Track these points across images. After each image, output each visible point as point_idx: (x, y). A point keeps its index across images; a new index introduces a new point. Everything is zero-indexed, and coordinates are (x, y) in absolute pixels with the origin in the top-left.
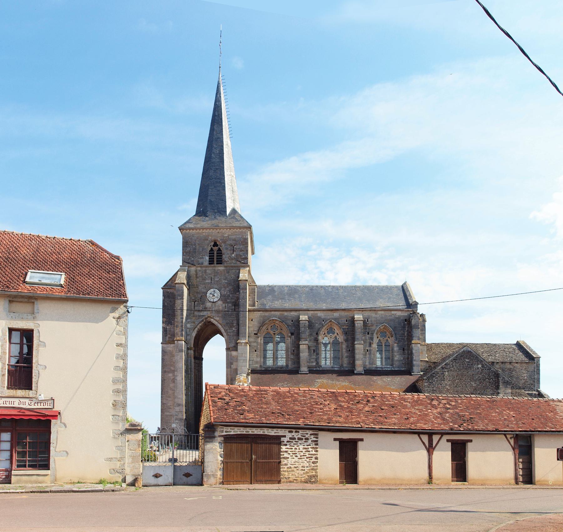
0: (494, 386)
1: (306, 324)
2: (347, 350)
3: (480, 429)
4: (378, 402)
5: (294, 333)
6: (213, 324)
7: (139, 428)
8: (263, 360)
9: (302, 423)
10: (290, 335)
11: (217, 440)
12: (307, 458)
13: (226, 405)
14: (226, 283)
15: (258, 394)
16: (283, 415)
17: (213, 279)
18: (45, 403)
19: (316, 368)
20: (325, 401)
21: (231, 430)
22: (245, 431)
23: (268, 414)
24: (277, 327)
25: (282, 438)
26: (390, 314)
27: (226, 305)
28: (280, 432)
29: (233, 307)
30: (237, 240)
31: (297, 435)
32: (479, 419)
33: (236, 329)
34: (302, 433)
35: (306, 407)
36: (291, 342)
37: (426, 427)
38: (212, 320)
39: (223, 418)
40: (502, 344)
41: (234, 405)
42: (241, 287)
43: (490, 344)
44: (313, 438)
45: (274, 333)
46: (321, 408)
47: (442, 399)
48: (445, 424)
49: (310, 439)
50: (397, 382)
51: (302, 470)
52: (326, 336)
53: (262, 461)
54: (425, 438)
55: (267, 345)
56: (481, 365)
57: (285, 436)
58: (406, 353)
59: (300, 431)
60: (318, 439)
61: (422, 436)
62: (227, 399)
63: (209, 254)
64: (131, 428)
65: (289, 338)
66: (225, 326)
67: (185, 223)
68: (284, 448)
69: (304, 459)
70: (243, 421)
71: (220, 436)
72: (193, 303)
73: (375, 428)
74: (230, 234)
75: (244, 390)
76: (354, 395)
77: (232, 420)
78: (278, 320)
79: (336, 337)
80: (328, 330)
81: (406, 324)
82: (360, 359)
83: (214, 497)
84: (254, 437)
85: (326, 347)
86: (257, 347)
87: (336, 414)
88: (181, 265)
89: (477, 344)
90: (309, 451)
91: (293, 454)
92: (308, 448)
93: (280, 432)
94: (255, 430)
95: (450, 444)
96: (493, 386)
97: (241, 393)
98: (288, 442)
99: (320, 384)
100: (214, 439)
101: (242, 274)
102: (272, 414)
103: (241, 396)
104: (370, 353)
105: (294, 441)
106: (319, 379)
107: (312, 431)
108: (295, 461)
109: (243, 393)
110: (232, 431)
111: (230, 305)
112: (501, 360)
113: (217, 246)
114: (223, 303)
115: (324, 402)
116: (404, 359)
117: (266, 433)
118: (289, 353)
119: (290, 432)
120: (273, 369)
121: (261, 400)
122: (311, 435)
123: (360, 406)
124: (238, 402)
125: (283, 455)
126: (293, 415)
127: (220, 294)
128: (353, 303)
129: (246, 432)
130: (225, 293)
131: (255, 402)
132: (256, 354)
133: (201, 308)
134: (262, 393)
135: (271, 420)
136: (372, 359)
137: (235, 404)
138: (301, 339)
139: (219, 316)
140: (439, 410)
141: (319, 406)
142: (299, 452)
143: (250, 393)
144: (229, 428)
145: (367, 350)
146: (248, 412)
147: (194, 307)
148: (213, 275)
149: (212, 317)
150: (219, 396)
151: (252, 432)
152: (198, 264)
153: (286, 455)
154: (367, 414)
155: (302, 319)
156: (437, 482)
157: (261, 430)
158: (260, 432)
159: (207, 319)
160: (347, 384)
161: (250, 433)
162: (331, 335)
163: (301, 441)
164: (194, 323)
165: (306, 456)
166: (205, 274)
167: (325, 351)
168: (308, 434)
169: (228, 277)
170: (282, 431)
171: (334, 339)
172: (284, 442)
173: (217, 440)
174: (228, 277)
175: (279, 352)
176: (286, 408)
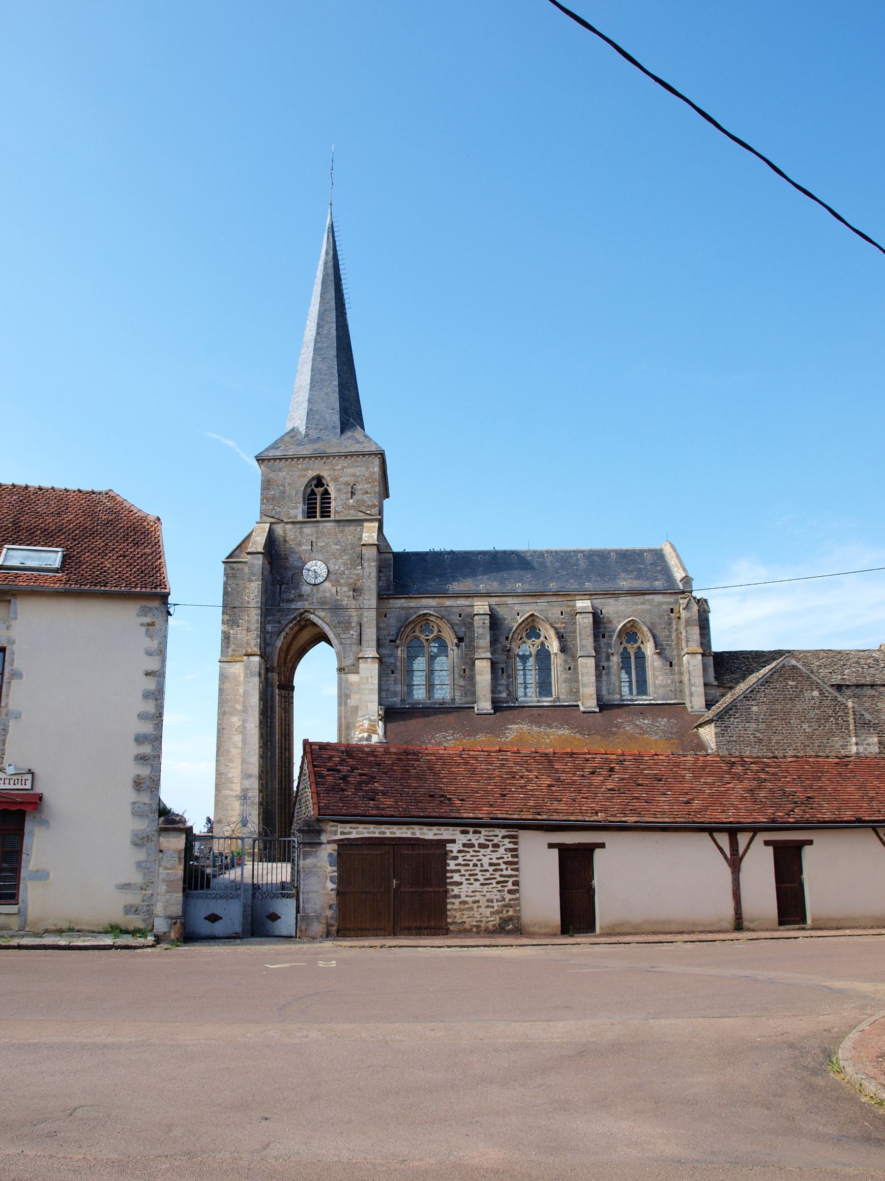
0: (846, 731)
1: (486, 622)
2: (565, 669)
3: (826, 819)
4: (631, 771)
5: (463, 638)
6: (315, 625)
7: (181, 826)
8: (407, 690)
9: (487, 816)
10: (456, 641)
11: (326, 849)
12: (498, 883)
13: (341, 781)
15: (400, 760)
16: (449, 799)
17: (314, 544)
18: (18, 779)
19: (507, 702)
20: (528, 771)
21: (351, 830)
22: (377, 831)
23: (421, 798)
24: (433, 627)
25: (447, 845)
26: (642, 600)
27: (338, 590)
28: (445, 833)
29: (351, 593)
30: (358, 475)
31: (477, 838)
32: (824, 800)
33: (356, 632)
34: (487, 833)
35: (493, 784)
36: (458, 654)
37: (723, 818)
38: (312, 617)
39: (335, 808)
40: (852, 651)
41: (356, 782)
42: (365, 557)
43: (831, 650)
44: (507, 844)
45: (427, 638)
46: (521, 784)
47: (752, 763)
48: (760, 811)
49: (503, 845)
50: (662, 728)
51: (488, 907)
52: (524, 642)
53: (411, 890)
54: (724, 840)
55: (414, 660)
56: (819, 691)
57: (453, 841)
58: (676, 671)
59: (482, 830)
60: (517, 845)
61: (716, 835)
62: (345, 769)
63: (309, 499)
64: (167, 826)
65: (455, 648)
66: (335, 628)
67: (267, 450)
68: (452, 865)
69: (490, 886)
70: (374, 812)
71: (329, 842)
72: (278, 586)
73: (626, 822)
74: (346, 465)
75: (376, 753)
76: (585, 758)
77: (353, 811)
78: (433, 615)
79: (542, 644)
80: (528, 631)
81: (673, 618)
82: (591, 685)
83: (321, 964)
84: (396, 844)
85: (524, 663)
87: (551, 797)
88: (258, 520)
89: (808, 652)
90: (502, 870)
91: (470, 875)
92: (499, 864)
93: (445, 833)
94: (398, 829)
95: (770, 849)
96: (843, 730)
97: (369, 758)
98: (459, 852)
99: (515, 734)
100: (320, 848)
101: (368, 534)
102: (430, 799)
103: (371, 765)
104: (609, 672)
105: (471, 850)
106: (514, 723)
107: (506, 830)
108: (474, 890)
109: (373, 759)
110: (354, 831)
111: (345, 589)
112: (854, 681)
113: (323, 485)
114: (332, 586)
115: (526, 773)
116: (672, 682)
117: (418, 835)
118: (456, 675)
119: (463, 832)
120: (425, 706)
121: (408, 771)
122: (503, 837)
123: (597, 780)
124: (365, 775)
125: (452, 877)
126: (469, 799)
127: (326, 570)
128: (573, 581)
129: (379, 833)
130: (337, 567)
131: (396, 776)
132: (393, 679)
133: (293, 596)
134: (409, 757)
135: (427, 810)
136: (613, 684)
137: (358, 780)
138: (478, 648)
140: (746, 784)
141: (517, 782)
142: (481, 871)
143: (386, 759)
144: (348, 826)
145: (603, 667)
146: (384, 794)
147: (280, 593)
148: (315, 536)
149: (311, 610)
150: (328, 764)
151: (391, 833)
152: (289, 519)
153: (457, 877)
154: (610, 795)
155: (478, 611)
156: (751, 926)
157: (408, 829)
158: (406, 833)
159: (303, 616)
160: (567, 732)
161: (388, 835)
162: (533, 641)
163: (486, 850)
164: (279, 622)
165: (495, 878)
166: (301, 536)
167: (524, 669)
168: (497, 836)
169: (342, 540)
170: (449, 832)
171: (539, 648)
172: (452, 852)
173: (326, 849)
174: (342, 540)
175: (436, 673)
176: (455, 786)
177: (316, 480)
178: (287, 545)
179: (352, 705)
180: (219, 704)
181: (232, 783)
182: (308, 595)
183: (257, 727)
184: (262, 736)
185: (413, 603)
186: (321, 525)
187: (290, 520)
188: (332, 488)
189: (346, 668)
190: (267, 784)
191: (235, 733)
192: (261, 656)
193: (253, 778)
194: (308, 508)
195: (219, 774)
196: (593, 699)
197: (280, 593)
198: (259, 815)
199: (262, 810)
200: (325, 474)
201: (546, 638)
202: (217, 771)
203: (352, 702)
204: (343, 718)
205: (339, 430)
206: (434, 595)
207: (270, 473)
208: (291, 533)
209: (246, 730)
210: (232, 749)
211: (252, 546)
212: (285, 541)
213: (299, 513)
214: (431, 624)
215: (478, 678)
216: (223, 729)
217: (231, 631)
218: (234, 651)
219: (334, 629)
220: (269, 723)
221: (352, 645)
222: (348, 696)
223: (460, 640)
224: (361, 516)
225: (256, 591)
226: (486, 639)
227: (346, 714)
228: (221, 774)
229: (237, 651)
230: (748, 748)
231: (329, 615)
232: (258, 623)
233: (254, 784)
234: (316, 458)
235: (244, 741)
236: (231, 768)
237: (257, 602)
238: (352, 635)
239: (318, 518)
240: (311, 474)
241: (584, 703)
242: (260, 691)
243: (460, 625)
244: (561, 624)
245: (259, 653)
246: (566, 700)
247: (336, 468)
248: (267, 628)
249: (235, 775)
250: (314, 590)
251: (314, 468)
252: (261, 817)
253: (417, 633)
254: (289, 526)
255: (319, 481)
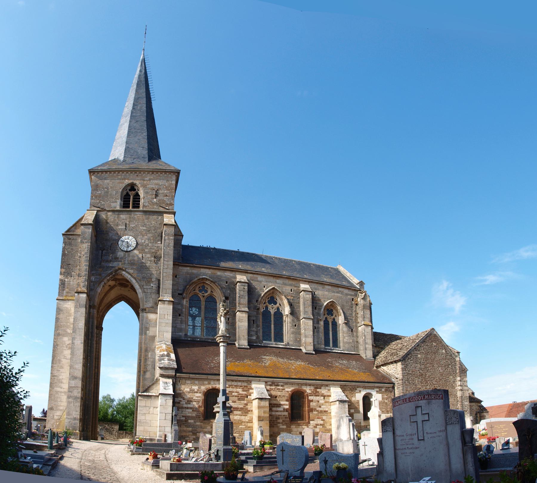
10: (224, 298)
14: (144, 230)
17: (127, 225)
24: (207, 288)
29: (153, 258)
63: (124, 198)
66: (140, 281)
72: (101, 251)
78: (209, 280)
86: (182, 310)
113: (135, 190)
120: (202, 340)
132: (180, 320)
133: (110, 258)
139: (134, 268)
147: (102, 256)
148: (128, 220)
149: (124, 268)
159: (117, 272)
164: (100, 275)
166: (118, 219)
174: (148, 224)
177: (130, 187)
178: (108, 225)
179: (150, 335)
180: (55, 328)
181: (62, 383)
182: (122, 258)
183: (82, 343)
184: (85, 351)
185: (195, 271)
186: (133, 213)
187: (111, 209)
188: (142, 191)
189: (147, 309)
190: (86, 385)
191: (65, 348)
192: (88, 296)
193: (78, 380)
194: (124, 204)
195: (53, 376)
196: (311, 346)
197: (102, 256)
198: (80, 406)
199: (82, 403)
200: (137, 182)
201: (280, 305)
202: (51, 373)
203: (150, 333)
204: (143, 344)
205: (147, 159)
206: (210, 267)
207: (98, 181)
208: (111, 218)
209: (74, 345)
210: (63, 360)
211: (85, 220)
212: (107, 223)
213: (117, 205)
214: (206, 286)
215: (238, 324)
216: (58, 345)
217: (66, 280)
218: (67, 293)
219: (139, 282)
220: (89, 343)
221: (152, 294)
222: (147, 329)
223: (227, 298)
224: (161, 209)
225: (86, 249)
226: (245, 299)
227: (145, 341)
228: (54, 376)
229: (70, 293)
230: (417, 379)
231: (136, 272)
232: (86, 271)
233: (79, 383)
234: (131, 172)
235: (72, 354)
236: (62, 372)
237: (87, 257)
238: (152, 287)
239: (131, 208)
240: (127, 182)
241: (306, 348)
242: (85, 318)
243: (226, 289)
244: (291, 297)
245: (86, 291)
246: (294, 345)
247: (145, 179)
248: (91, 278)
249: (64, 377)
250: (126, 255)
251: (130, 178)
252: (81, 408)
253: (197, 291)
254: (110, 213)
255: (132, 187)
